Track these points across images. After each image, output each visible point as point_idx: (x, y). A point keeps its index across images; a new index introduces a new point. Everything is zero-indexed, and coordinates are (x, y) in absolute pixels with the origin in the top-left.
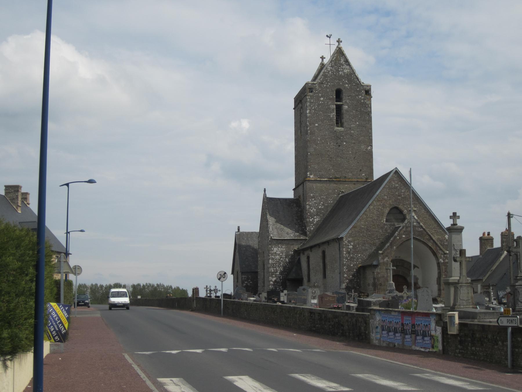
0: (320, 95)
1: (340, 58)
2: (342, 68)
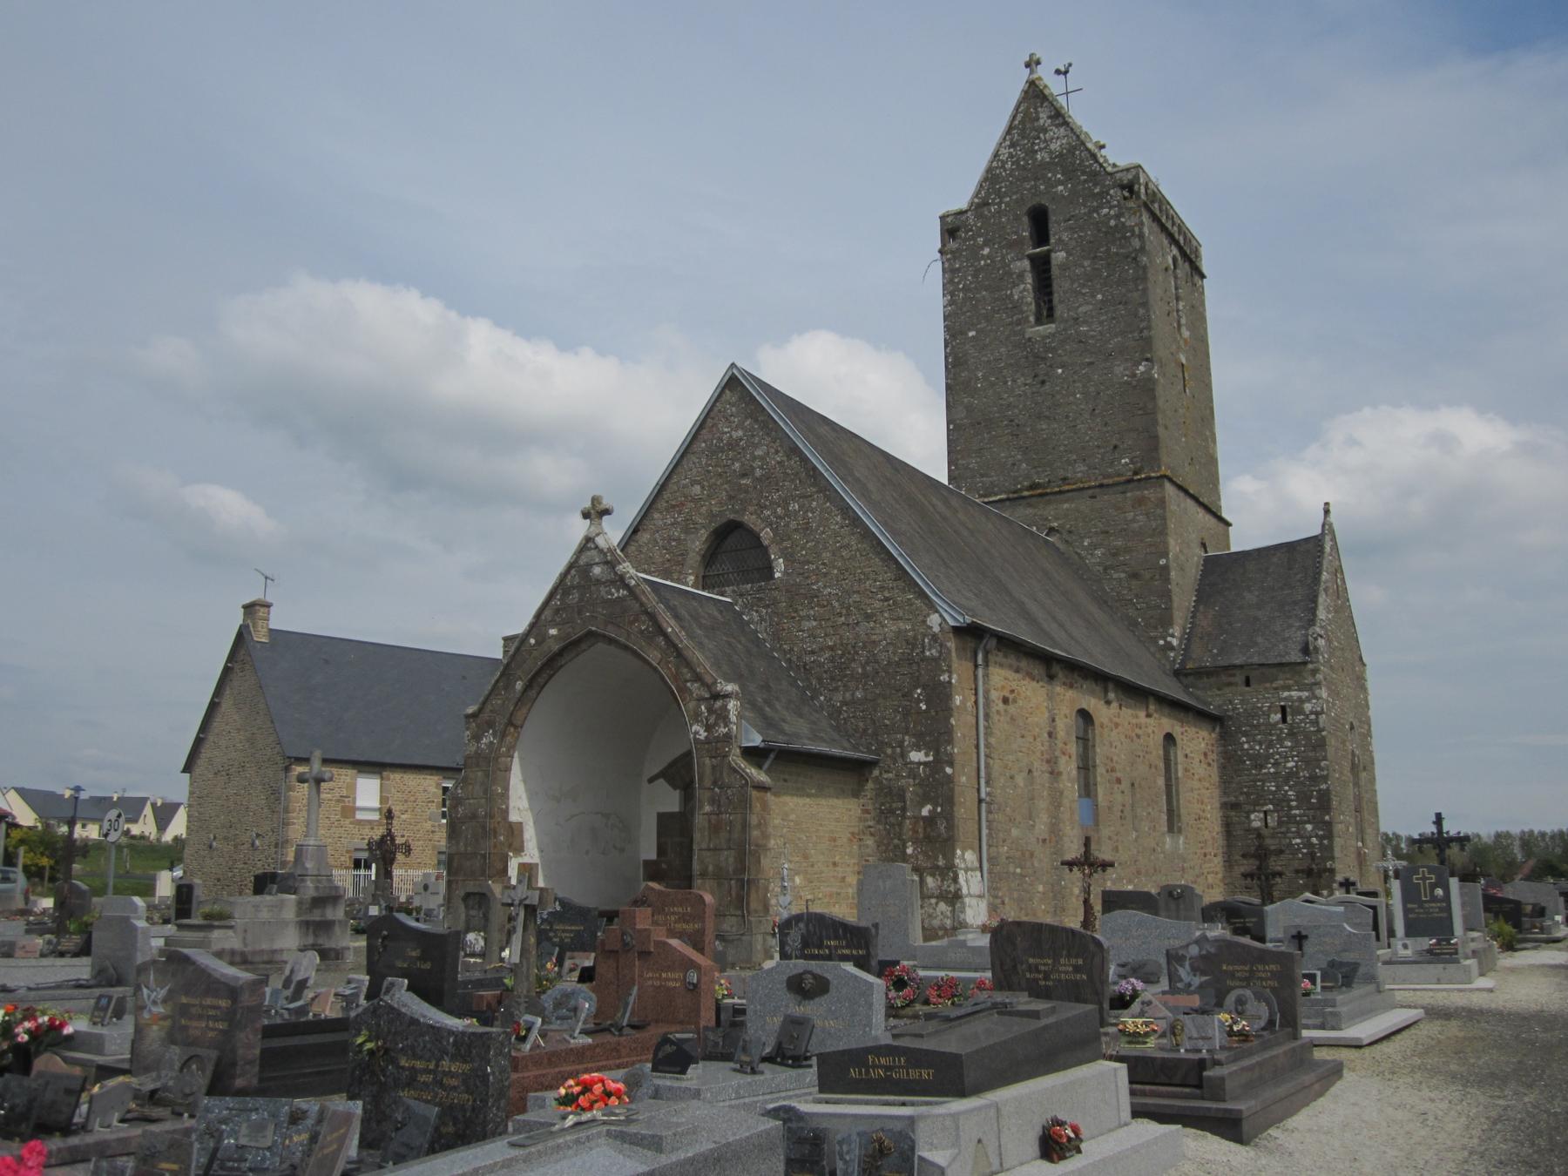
0: (980, 240)
1: (1037, 113)
2: (1045, 141)
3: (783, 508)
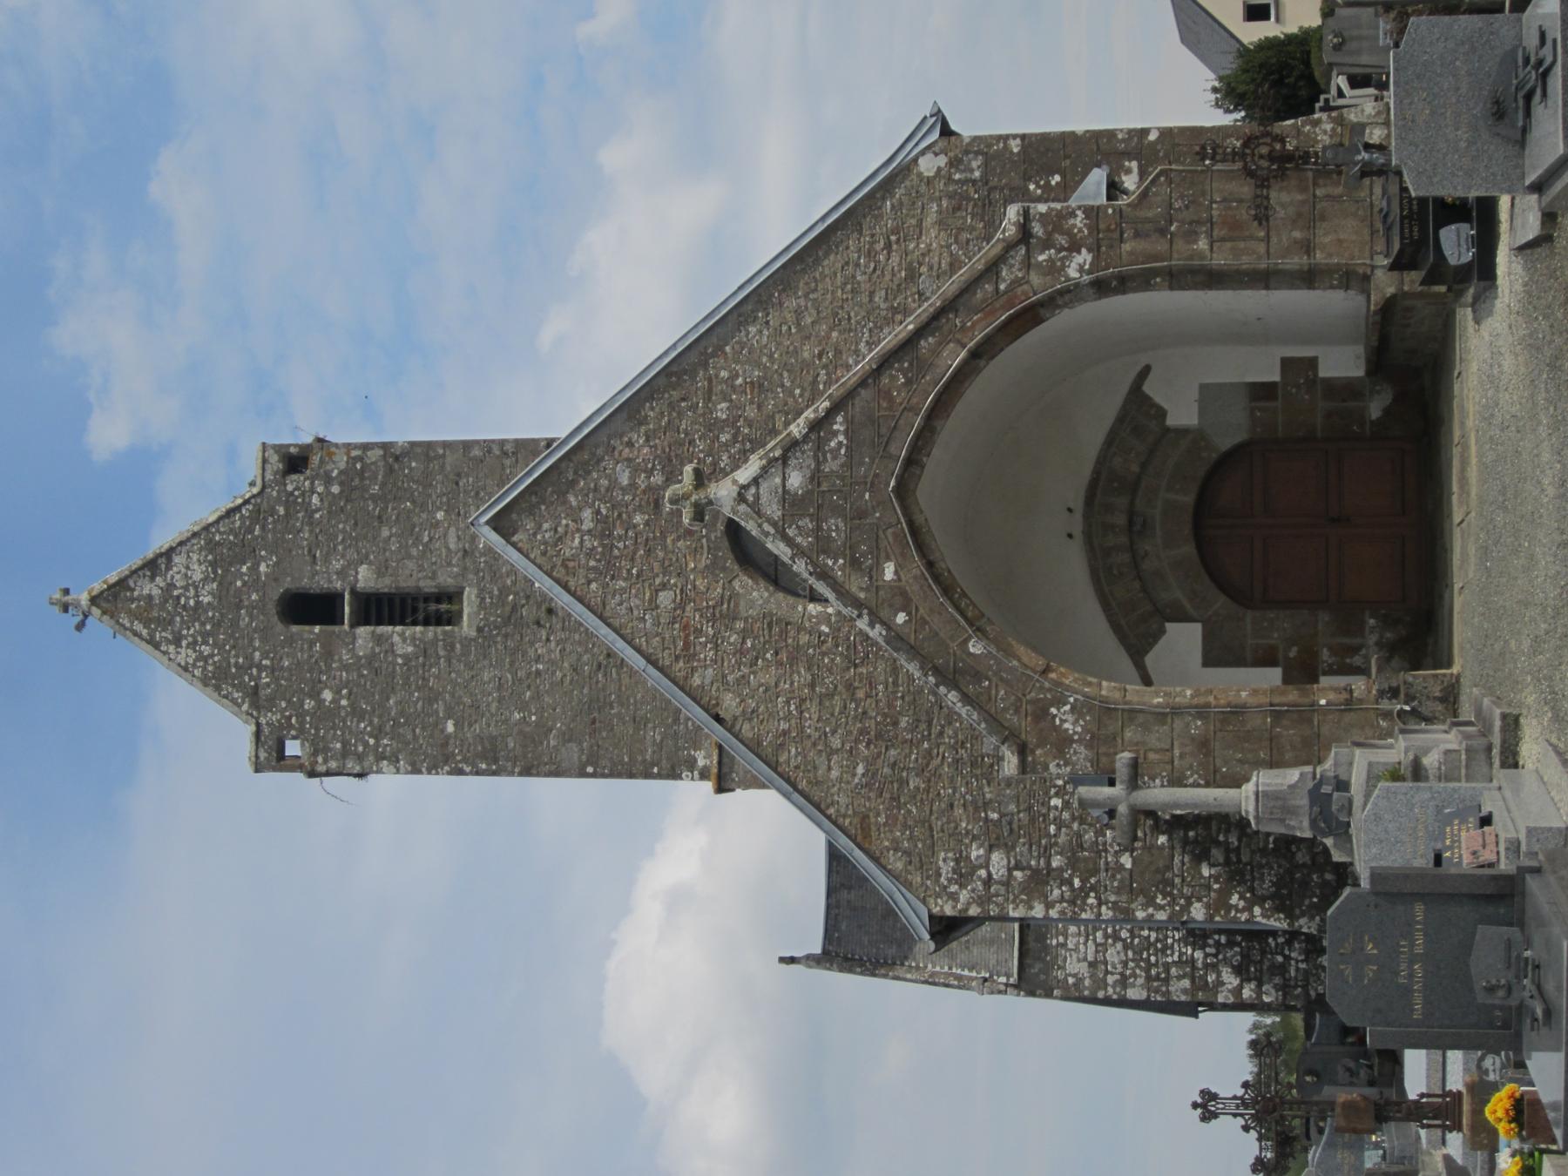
0: (309, 704)
1: (138, 599)
2: (186, 588)
3: (722, 430)
